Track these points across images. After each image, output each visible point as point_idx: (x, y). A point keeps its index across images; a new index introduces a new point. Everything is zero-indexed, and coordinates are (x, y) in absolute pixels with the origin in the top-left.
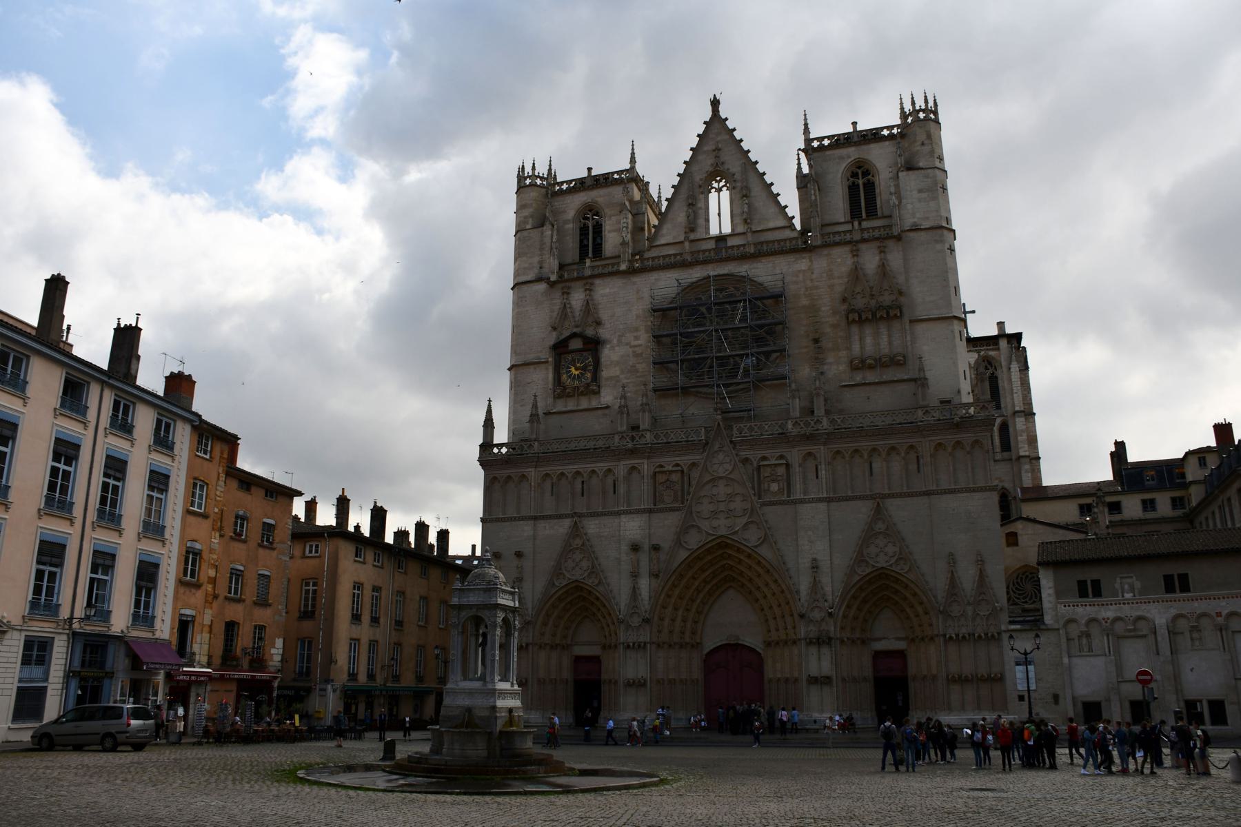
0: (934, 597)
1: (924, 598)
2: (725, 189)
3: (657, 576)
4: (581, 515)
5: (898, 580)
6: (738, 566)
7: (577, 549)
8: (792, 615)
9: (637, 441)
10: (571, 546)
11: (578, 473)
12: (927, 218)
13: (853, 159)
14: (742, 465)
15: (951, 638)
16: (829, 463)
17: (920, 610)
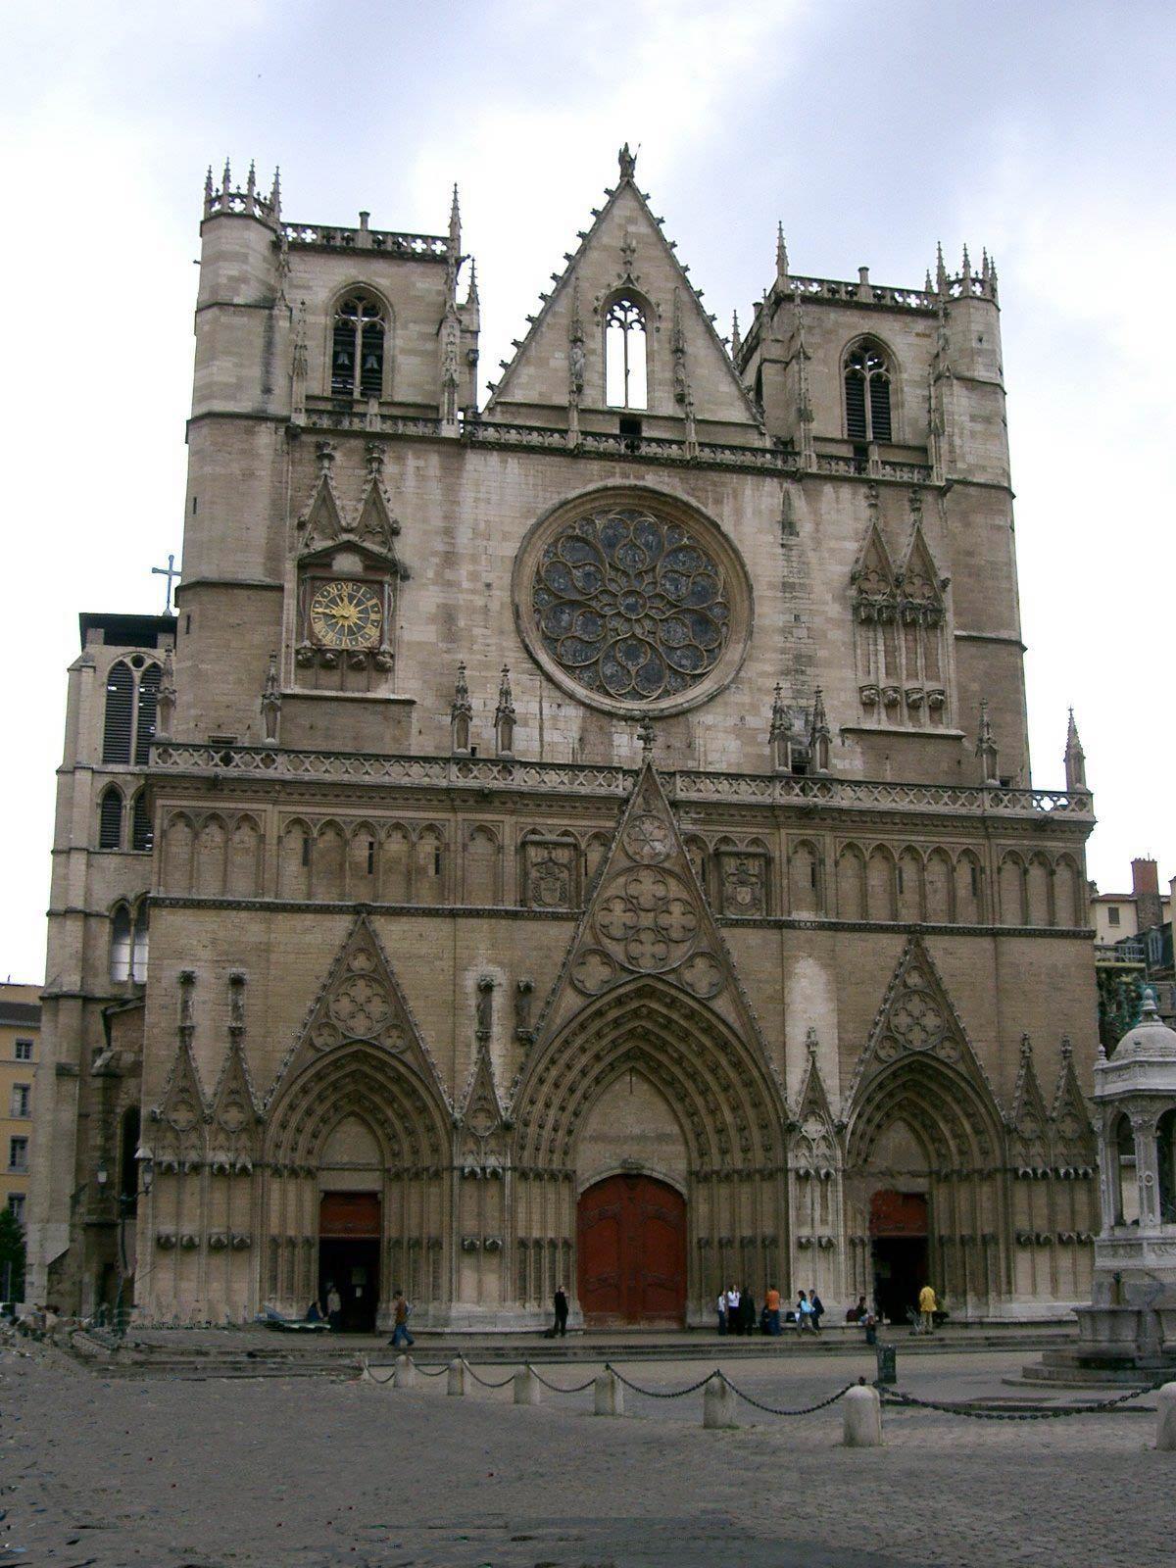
2: (637, 326)
4: (372, 911)
6: (664, 1034)
7: (362, 976)
10: (349, 970)
11: (366, 825)
12: (984, 468)
13: (857, 333)
15: (1025, 1174)
16: (837, 863)
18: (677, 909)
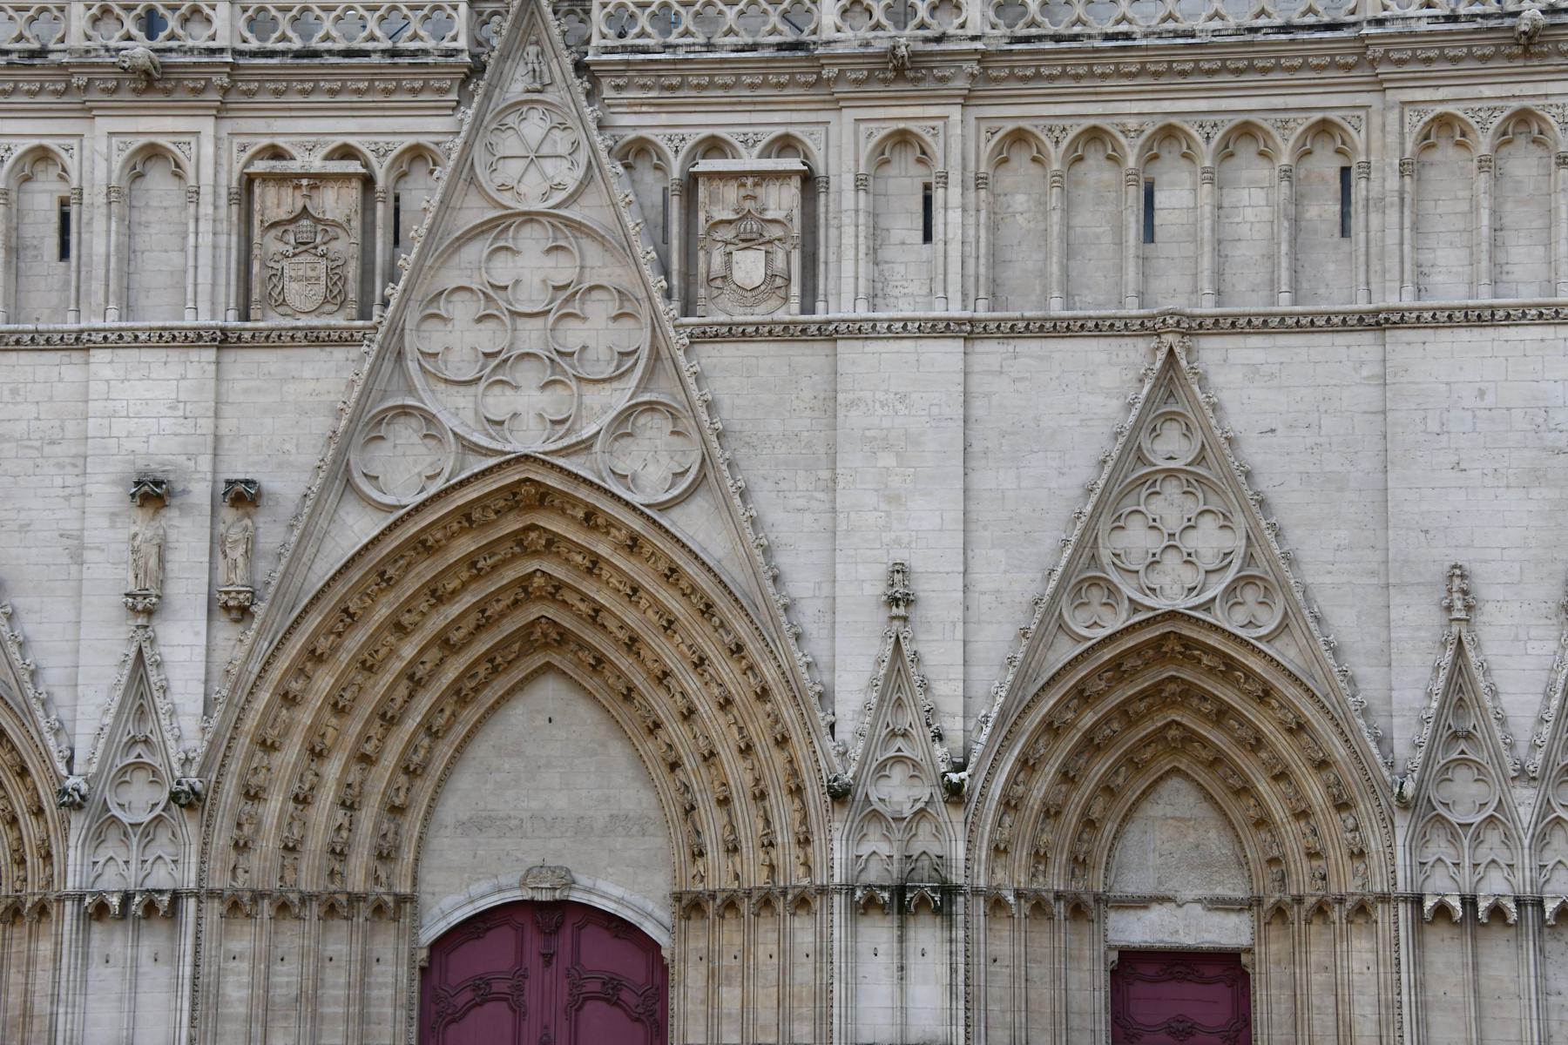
0: (1379, 741)
1: (1337, 741)
3: (243, 613)
5: (1230, 664)
6: (589, 587)
8: (797, 791)
9: (172, 37)
14: (620, 169)
15: (1442, 910)
17: (1314, 789)
18: (600, 309)
